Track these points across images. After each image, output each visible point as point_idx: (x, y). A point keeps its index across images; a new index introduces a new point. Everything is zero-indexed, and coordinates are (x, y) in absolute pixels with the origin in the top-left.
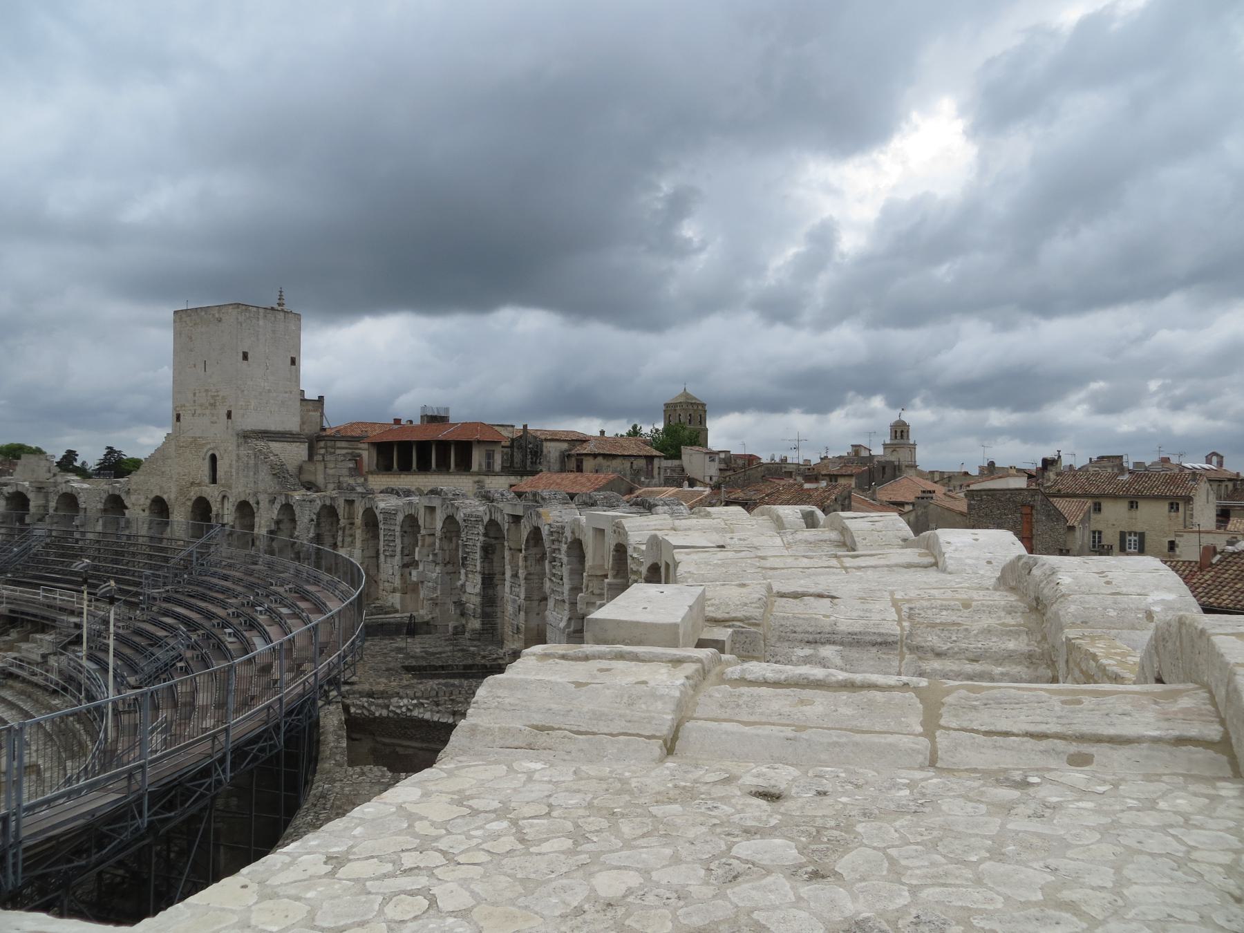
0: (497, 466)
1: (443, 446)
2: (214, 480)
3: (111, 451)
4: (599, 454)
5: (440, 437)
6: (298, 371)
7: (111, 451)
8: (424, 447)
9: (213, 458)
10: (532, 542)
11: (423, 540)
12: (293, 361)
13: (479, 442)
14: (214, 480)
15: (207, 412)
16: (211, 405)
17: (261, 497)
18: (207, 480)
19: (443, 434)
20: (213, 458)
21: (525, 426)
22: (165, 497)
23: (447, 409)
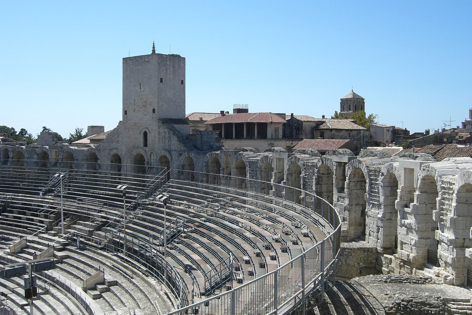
0: (280, 136)
1: (250, 125)
2: (146, 145)
3: (45, 128)
4: (334, 129)
5: (249, 121)
6: (184, 87)
7: (45, 128)
8: (239, 126)
9: (145, 134)
10: (352, 176)
11: (275, 176)
12: (183, 82)
13: (272, 123)
14: (146, 145)
15: (142, 109)
16: (144, 106)
17: (173, 153)
18: (142, 145)
19: (241, 119)
20: (145, 134)
21: (292, 114)
22: (119, 154)
23: (247, 105)
